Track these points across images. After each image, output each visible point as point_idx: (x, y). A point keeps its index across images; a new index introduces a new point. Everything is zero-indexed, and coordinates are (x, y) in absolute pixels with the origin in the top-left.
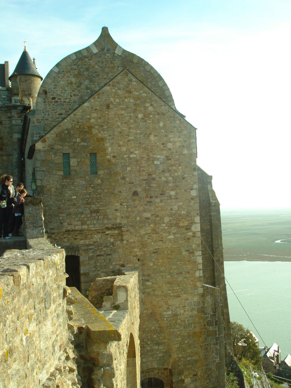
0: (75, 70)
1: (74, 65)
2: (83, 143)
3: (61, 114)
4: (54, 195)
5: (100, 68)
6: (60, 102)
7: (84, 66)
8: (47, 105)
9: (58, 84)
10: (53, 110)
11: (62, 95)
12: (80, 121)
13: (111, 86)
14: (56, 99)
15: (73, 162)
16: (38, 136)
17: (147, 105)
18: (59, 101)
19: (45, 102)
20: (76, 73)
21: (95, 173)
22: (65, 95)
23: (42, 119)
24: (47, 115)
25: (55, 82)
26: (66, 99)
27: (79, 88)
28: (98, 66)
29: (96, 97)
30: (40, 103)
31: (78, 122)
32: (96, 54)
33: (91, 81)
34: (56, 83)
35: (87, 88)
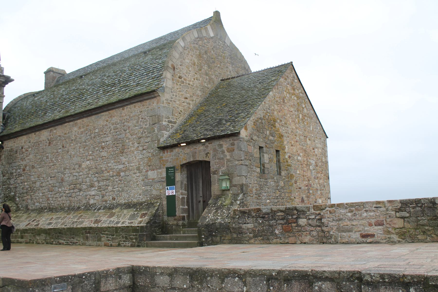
0: (197, 49)
1: (197, 44)
2: (271, 138)
3: (186, 98)
4: (256, 197)
5: (215, 55)
6: (185, 83)
7: (203, 48)
8: (175, 83)
9: (184, 61)
10: (180, 92)
11: (187, 75)
12: (268, 111)
13: (284, 79)
14: (182, 79)
15: (266, 157)
16: (167, 120)
17: (304, 106)
18: (185, 81)
19: (173, 80)
20: (198, 53)
21: (280, 174)
22: (190, 77)
23: (171, 99)
24: (174, 96)
25: (181, 58)
26: (190, 81)
27: (200, 72)
28: (214, 51)
29: (276, 87)
30: (169, 79)
31: (267, 112)
32: (212, 38)
33: (209, 67)
34: (182, 59)
35: (207, 74)
